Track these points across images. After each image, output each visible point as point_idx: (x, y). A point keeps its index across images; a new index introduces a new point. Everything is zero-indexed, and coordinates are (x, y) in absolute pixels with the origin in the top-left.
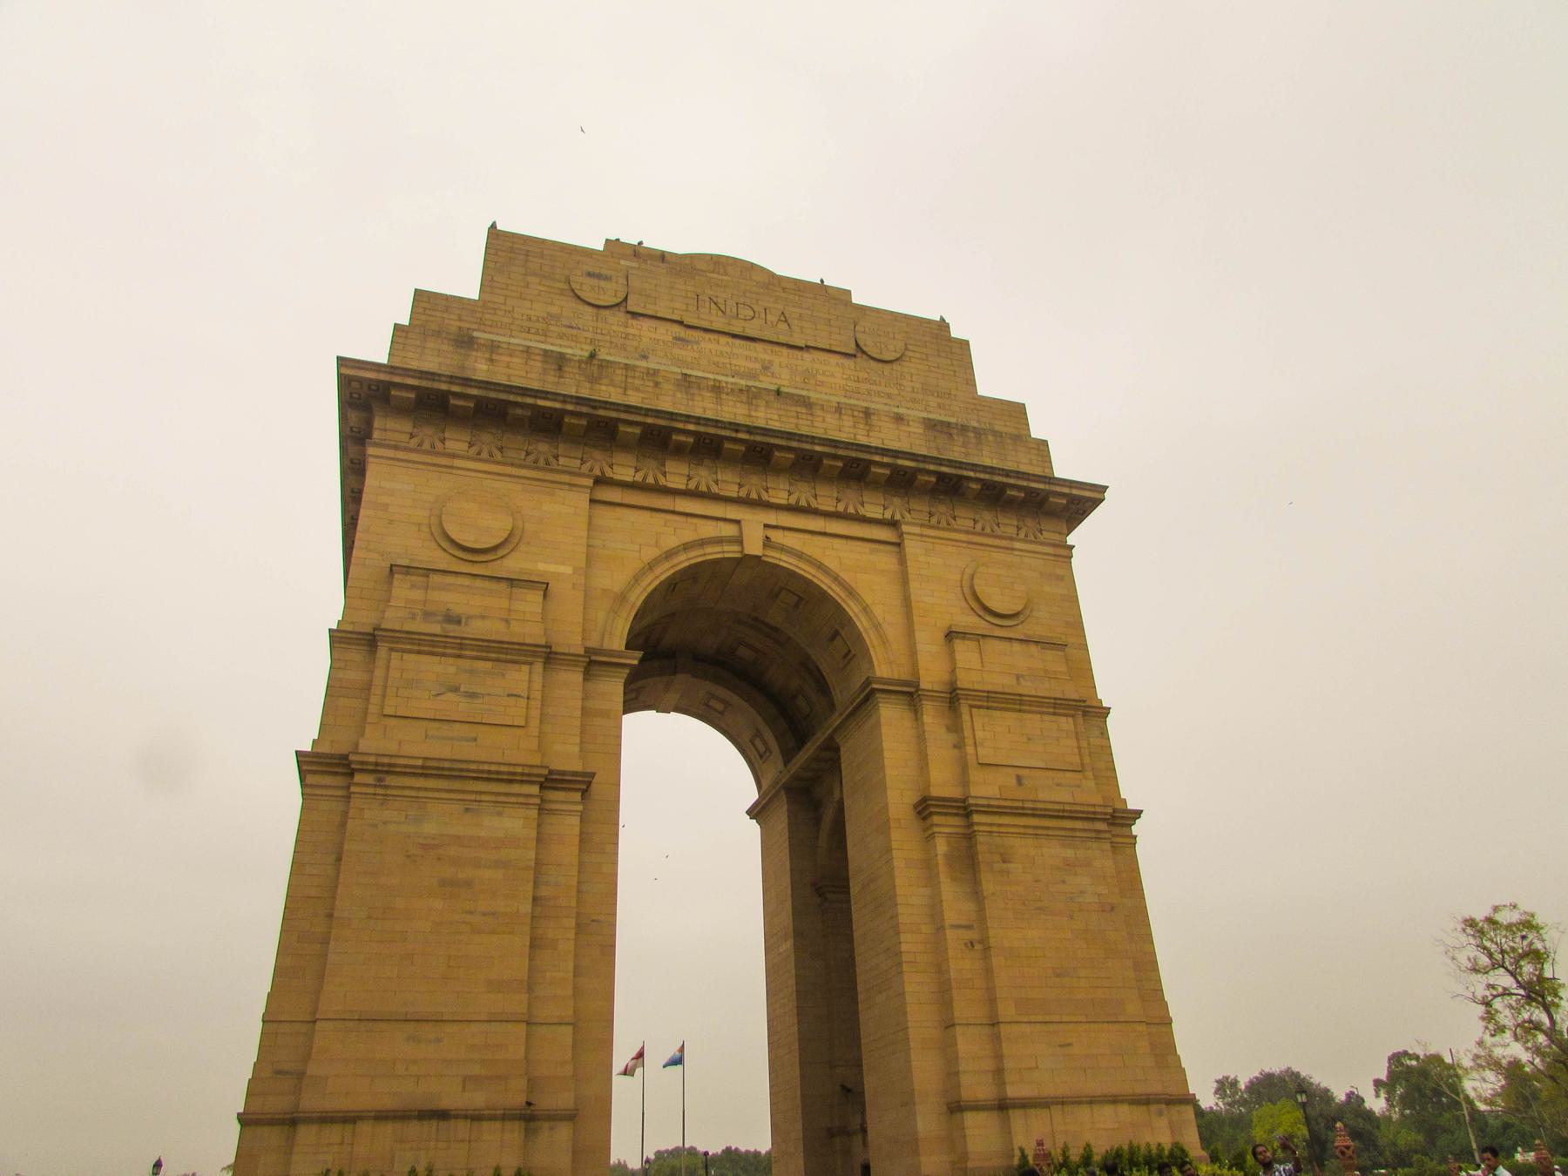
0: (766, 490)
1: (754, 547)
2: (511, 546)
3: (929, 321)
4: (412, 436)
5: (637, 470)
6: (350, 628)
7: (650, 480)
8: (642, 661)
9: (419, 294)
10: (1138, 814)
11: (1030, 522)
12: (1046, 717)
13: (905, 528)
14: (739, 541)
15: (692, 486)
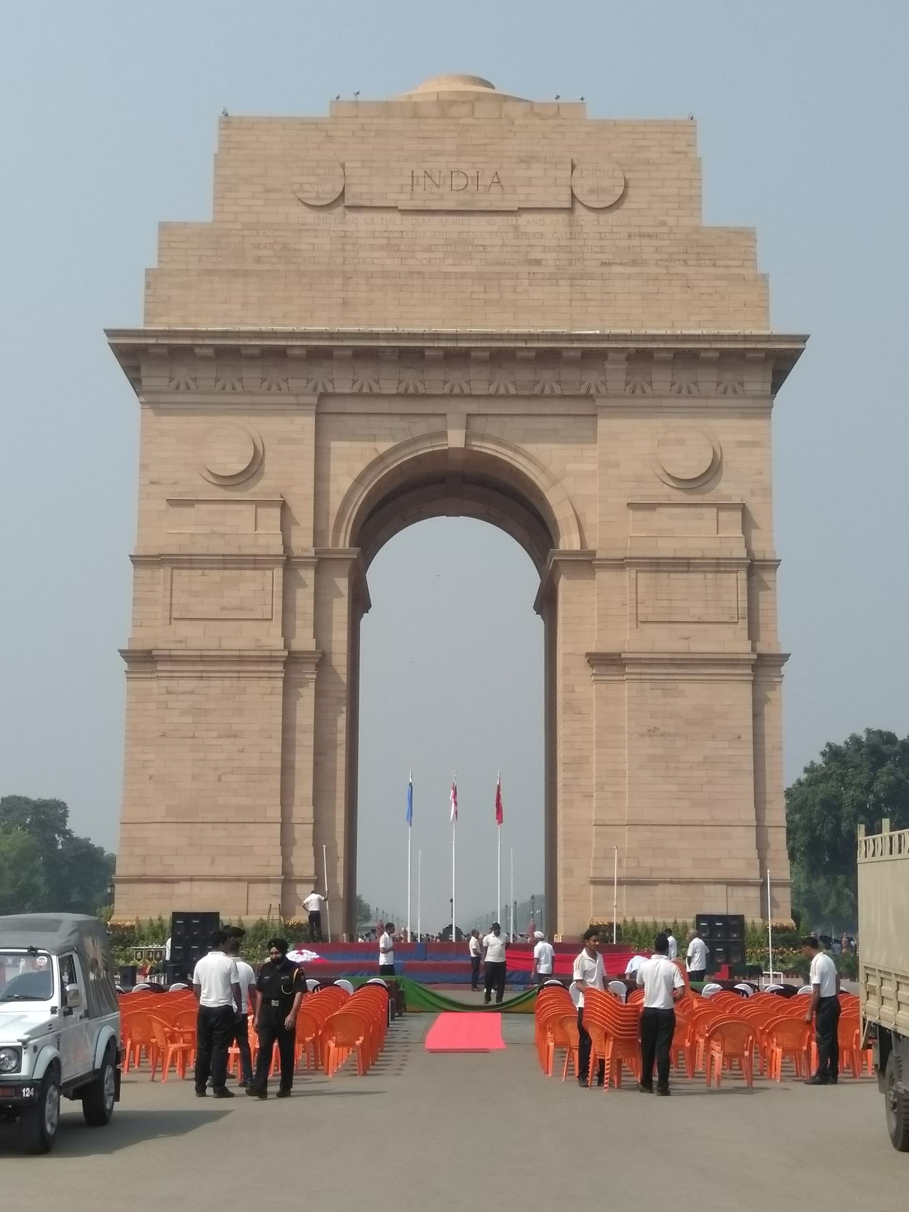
0: (469, 382)
1: (455, 439)
2: (255, 468)
3: (674, 123)
4: (171, 379)
5: (354, 382)
6: (142, 553)
7: (365, 390)
8: (358, 555)
9: (164, 227)
10: (786, 657)
11: (729, 377)
12: (710, 576)
13: (599, 402)
14: (443, 435)
15: (402, 390)
